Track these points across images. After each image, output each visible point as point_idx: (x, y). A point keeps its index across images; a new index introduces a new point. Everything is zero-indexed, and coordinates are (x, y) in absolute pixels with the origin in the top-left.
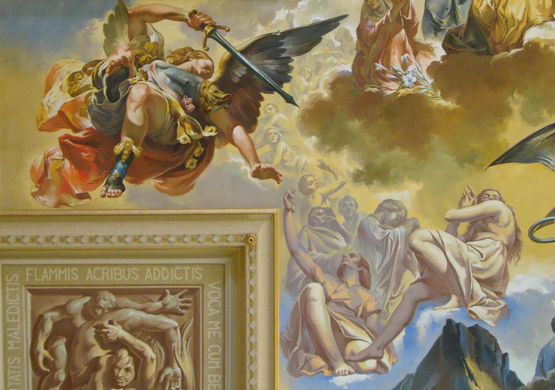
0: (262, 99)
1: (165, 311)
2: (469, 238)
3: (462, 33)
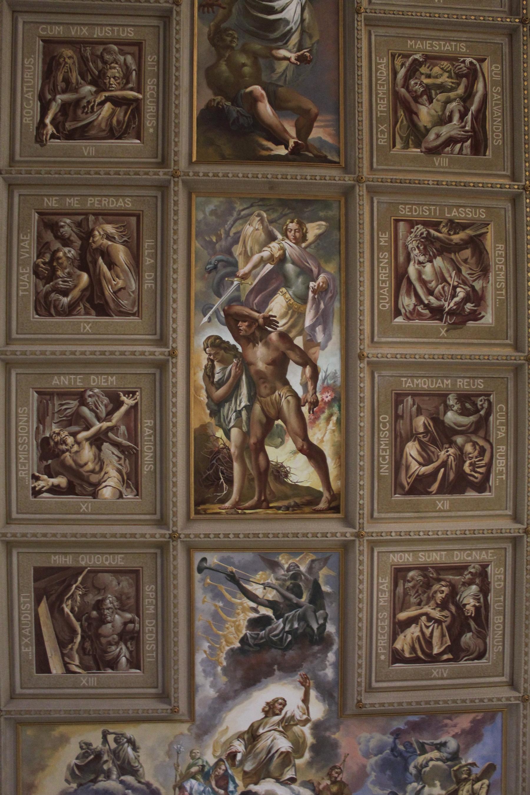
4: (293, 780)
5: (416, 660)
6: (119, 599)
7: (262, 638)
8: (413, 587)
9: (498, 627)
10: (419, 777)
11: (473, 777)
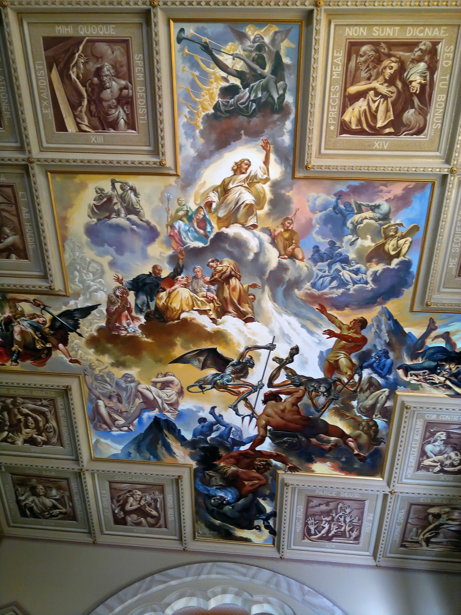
0: (69, 334)
1: (42, 405)
2: (162, 389)
3: (152, 313)
4: (255, 226)
5: (362, 132)
6: (114, 67)
7: (231, 106)
8: (365, 62)
9: (440, 105)
10: (355, 231)
11: (399, 234)
